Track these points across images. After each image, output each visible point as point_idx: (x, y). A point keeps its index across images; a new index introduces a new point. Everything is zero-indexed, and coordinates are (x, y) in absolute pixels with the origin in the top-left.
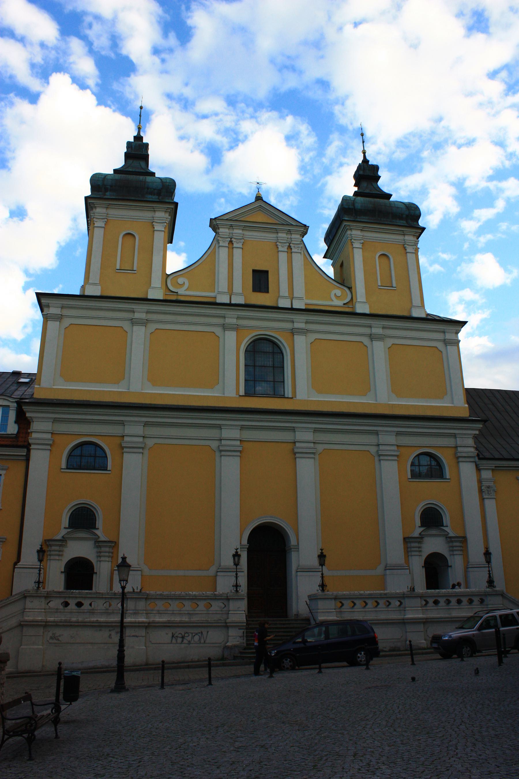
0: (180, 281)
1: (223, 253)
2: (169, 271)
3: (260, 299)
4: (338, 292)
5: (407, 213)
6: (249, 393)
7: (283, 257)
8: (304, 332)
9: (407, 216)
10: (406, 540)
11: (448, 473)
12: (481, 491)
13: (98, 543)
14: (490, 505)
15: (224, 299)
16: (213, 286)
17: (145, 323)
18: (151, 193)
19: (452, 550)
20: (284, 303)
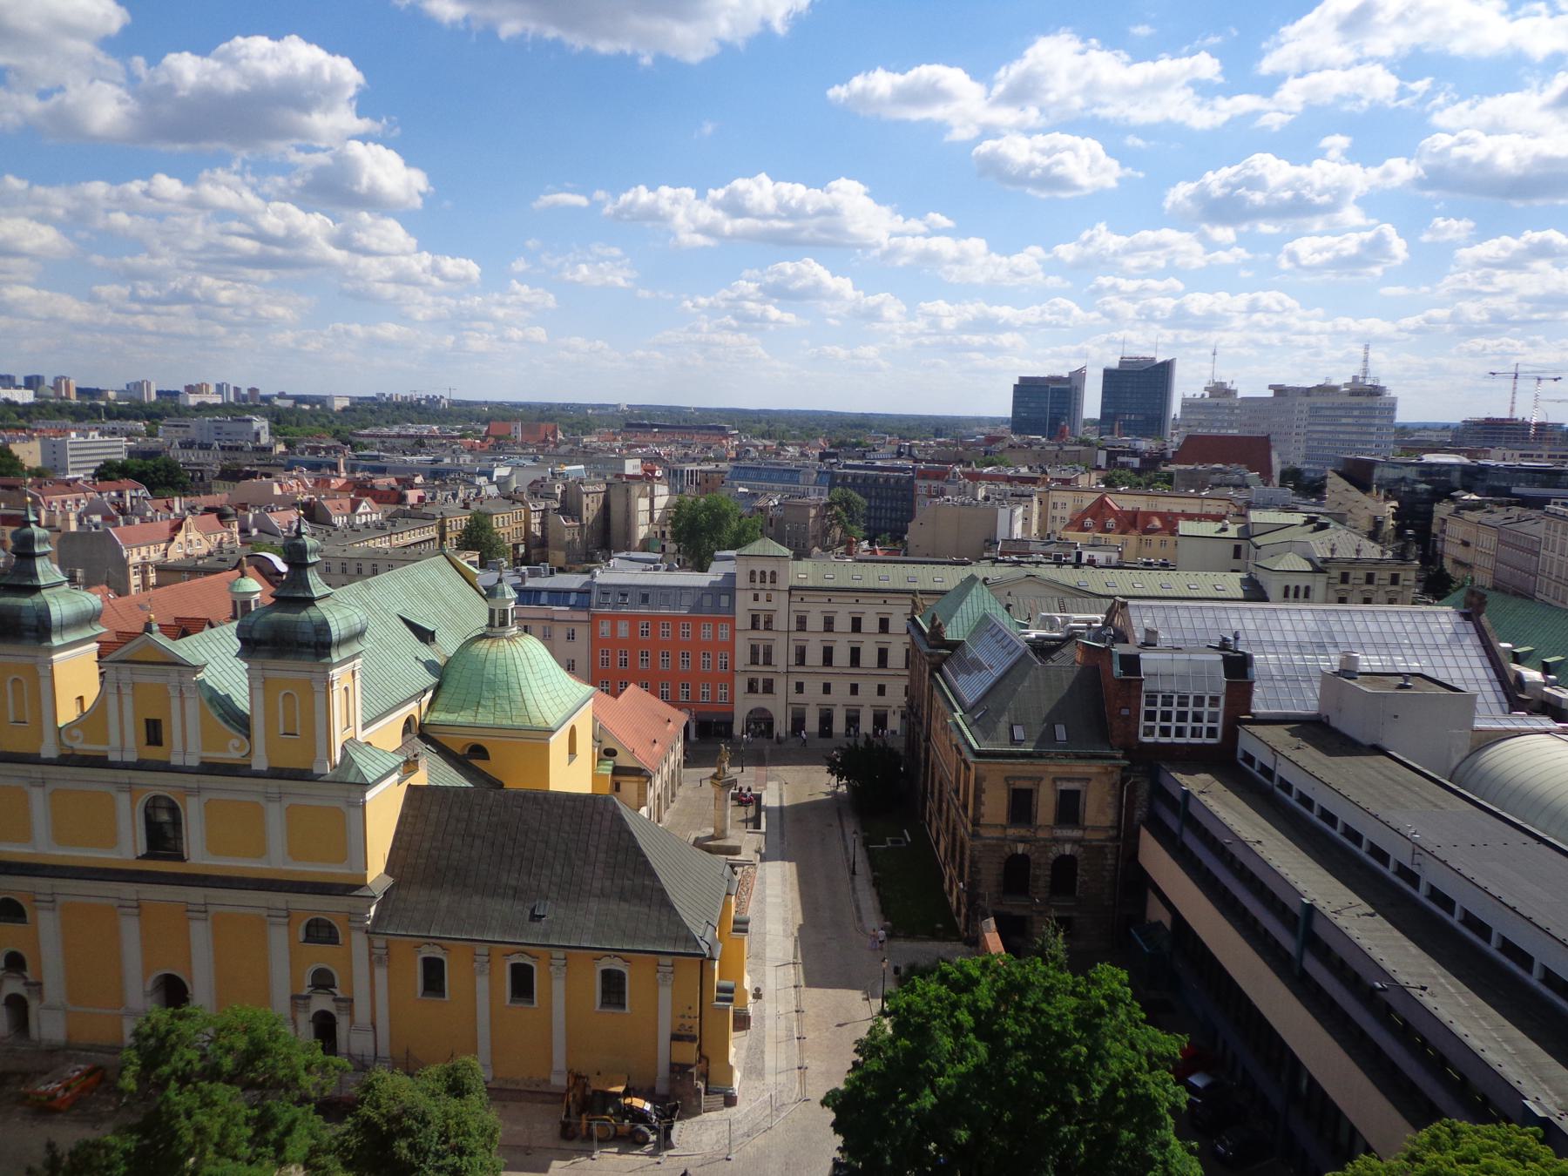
0: (75, 732)
1: (112, 701)
2: (60, 725)
3: (154, 753)
4: (236, 743)
5: (314, 639)
6: (144, 857)
7: (175, 704)
8: (198, 791)
9: (316, 643)
10: (294, 998)
11: (341, 940)
12: (371, 963)
13: (26, 984)
14: (381, 974)
15: (114, 757)
16: (106, 742)
17: (43, 783)
18: (30, 630)
19: (338, 1009)
20: (176, 760)
